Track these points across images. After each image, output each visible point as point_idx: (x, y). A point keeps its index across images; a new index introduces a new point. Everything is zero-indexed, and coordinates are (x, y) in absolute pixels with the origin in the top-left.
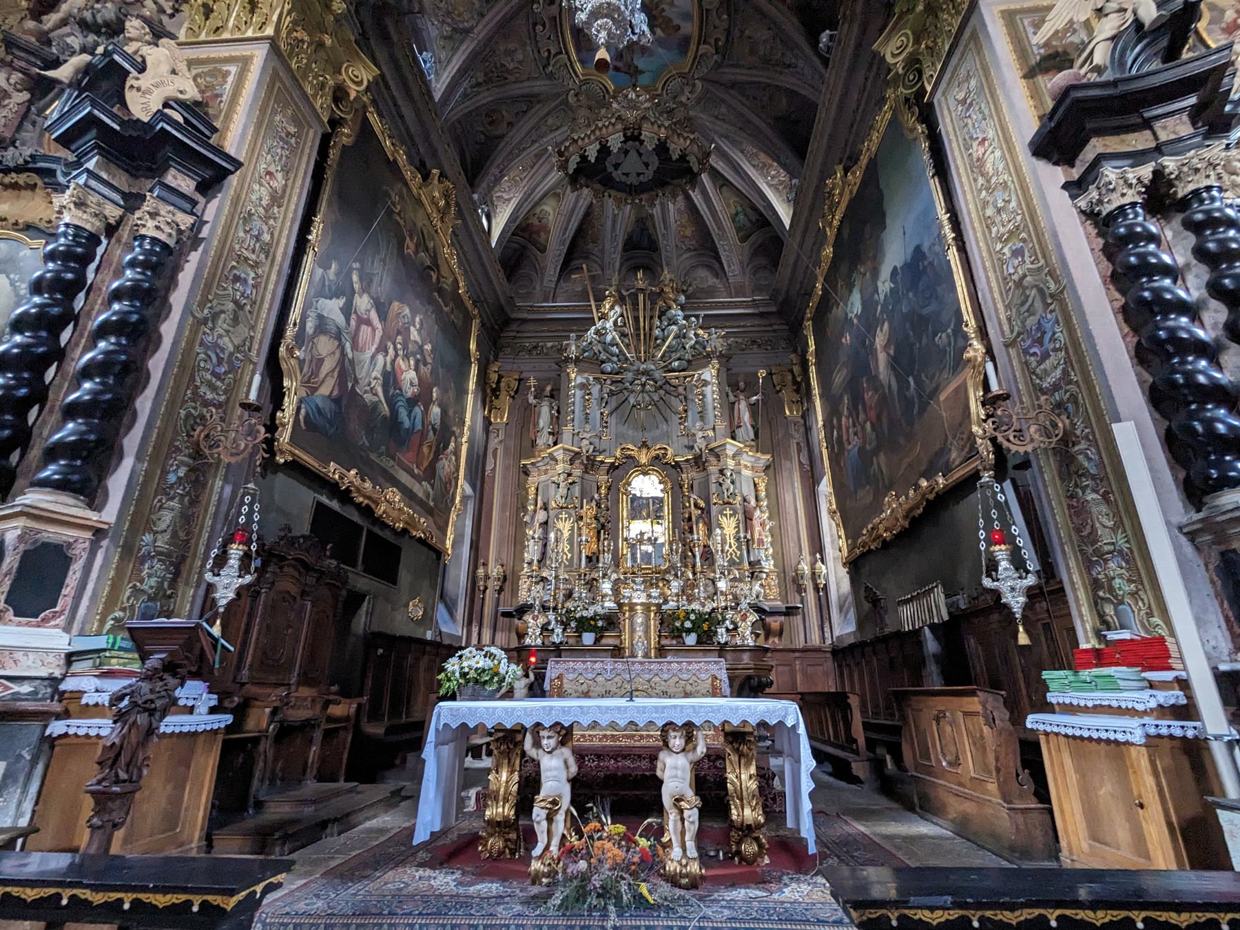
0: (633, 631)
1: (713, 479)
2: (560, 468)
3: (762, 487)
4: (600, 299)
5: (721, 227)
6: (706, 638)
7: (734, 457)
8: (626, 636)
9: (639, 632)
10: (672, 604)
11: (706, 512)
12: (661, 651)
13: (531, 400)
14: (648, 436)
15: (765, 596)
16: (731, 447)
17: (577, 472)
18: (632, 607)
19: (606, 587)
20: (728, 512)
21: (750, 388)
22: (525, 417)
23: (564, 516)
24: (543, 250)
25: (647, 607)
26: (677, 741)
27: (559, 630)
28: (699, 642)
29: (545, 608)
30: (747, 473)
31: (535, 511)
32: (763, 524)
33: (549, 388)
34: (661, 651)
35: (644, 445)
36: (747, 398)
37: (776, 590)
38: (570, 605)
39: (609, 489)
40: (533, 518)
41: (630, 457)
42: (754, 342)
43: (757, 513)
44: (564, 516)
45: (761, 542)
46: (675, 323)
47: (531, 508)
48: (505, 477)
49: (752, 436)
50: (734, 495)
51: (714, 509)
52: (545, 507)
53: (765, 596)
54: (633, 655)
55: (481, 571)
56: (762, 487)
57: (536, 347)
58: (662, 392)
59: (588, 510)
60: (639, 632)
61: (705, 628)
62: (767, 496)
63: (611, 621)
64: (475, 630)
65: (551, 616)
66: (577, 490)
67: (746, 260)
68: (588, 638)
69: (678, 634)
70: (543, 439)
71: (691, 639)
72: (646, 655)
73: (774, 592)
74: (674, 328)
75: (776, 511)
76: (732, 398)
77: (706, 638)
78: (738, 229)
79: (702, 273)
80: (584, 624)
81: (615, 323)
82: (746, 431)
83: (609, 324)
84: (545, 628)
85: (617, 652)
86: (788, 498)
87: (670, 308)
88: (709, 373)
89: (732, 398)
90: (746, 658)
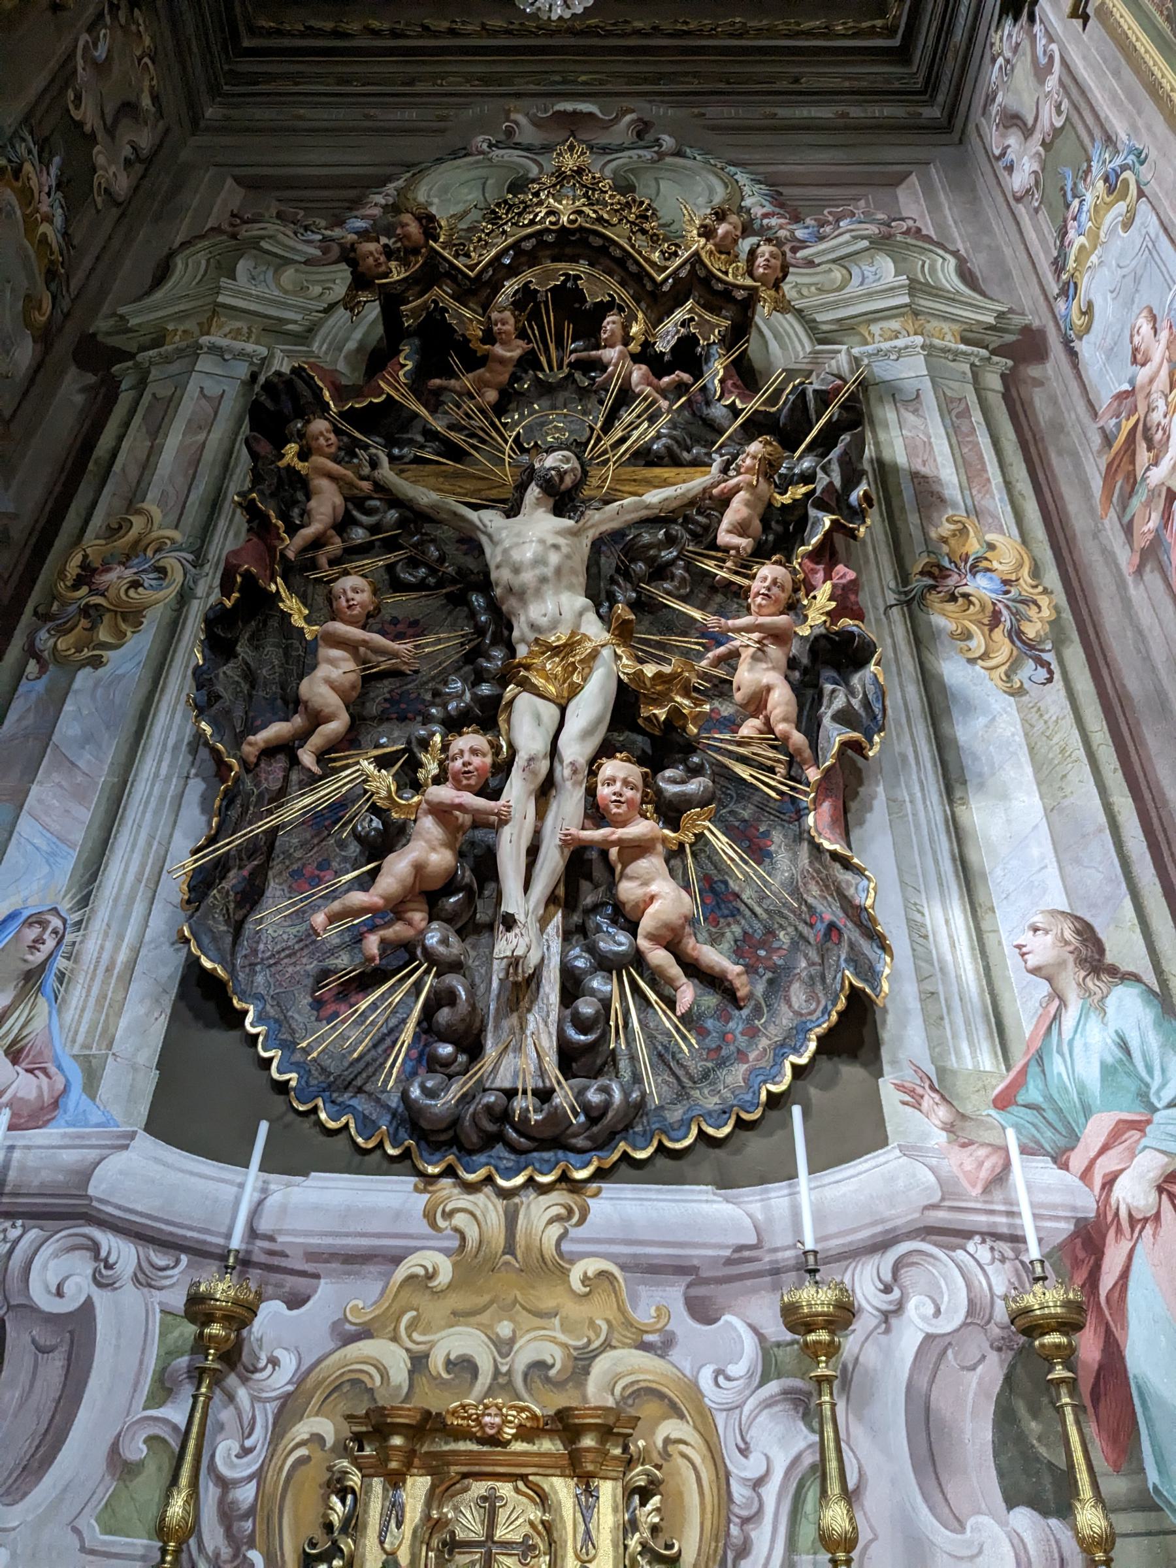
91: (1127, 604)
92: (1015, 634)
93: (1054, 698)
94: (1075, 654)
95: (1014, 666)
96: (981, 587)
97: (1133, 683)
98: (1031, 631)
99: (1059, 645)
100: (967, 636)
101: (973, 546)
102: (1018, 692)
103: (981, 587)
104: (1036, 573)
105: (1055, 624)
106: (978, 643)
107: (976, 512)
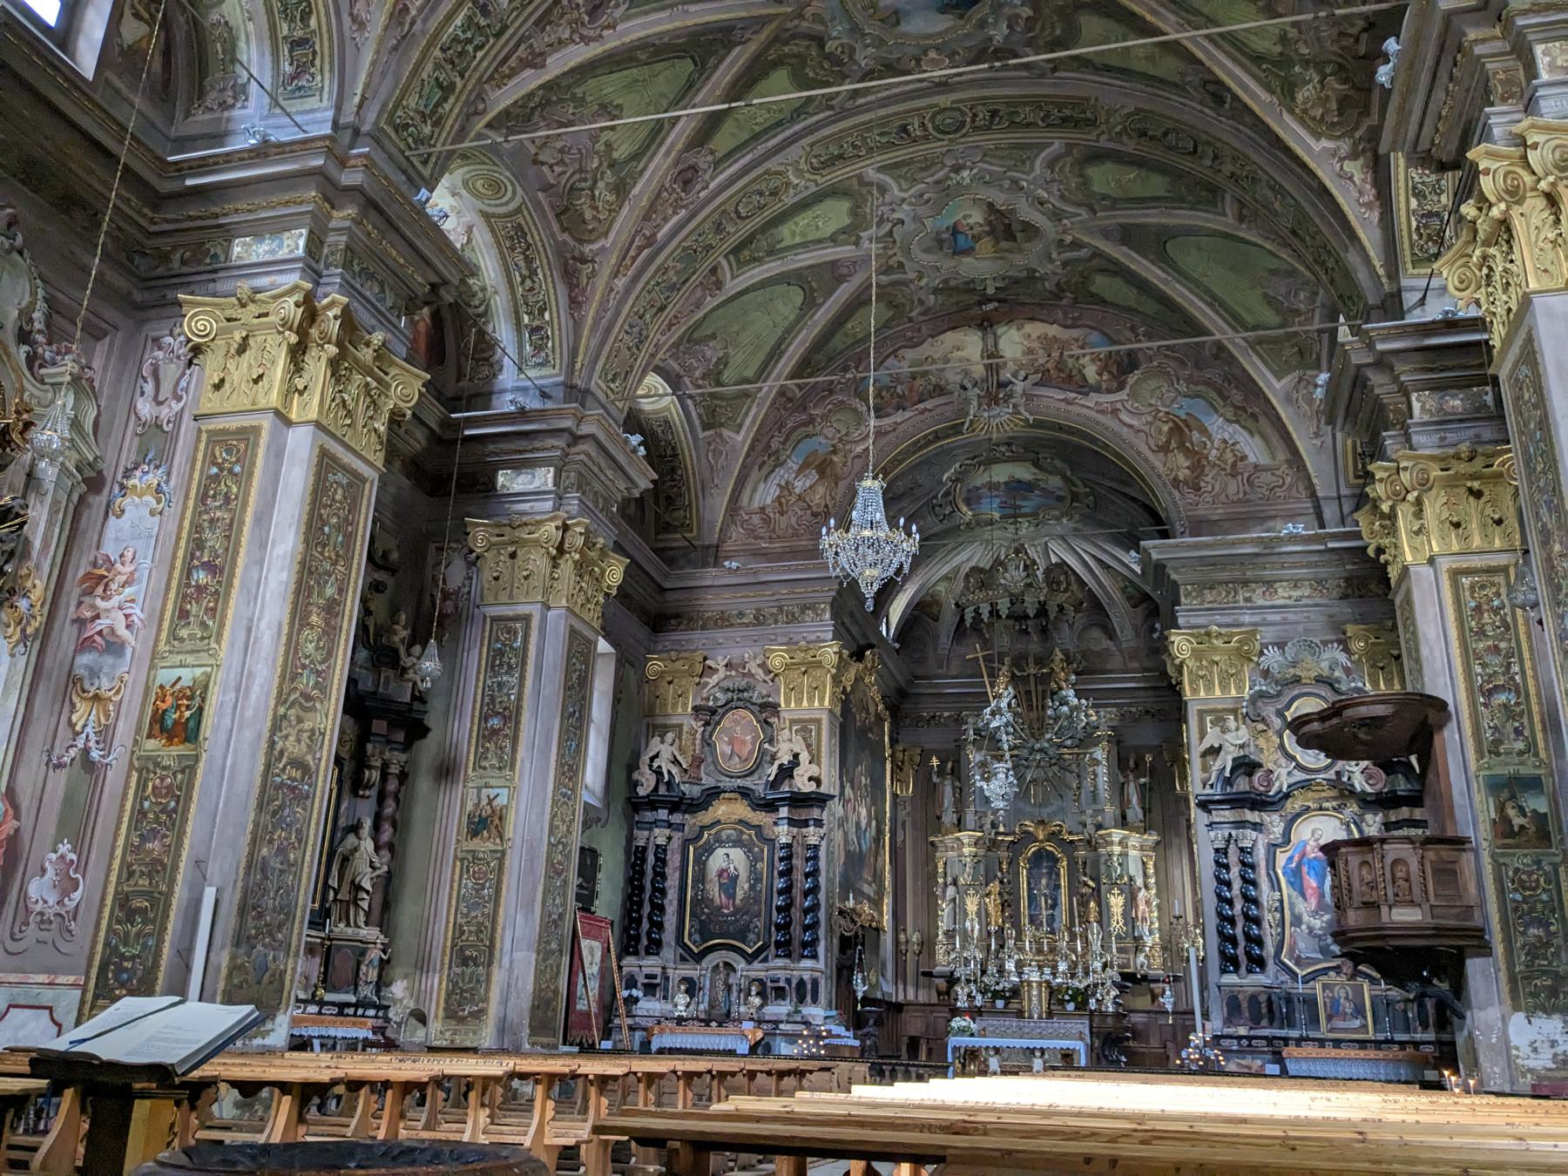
0: (1030, 1000)
1: (1102, 860)
2: (966, 850)
3: (1151, 864)
4: (993, 675)
5: (1110, 598)
6: (1082, 1005)
7: (1120, 843)
8: (1026, 1003)
9: (1035, 1001)
10: (1059, 980)
11: (1097, 890)
12: (1050, 1015)
13: (935, 779)
14: (1046, 811)
15: (1149, 967)
16: (1117, 834)
17: (982, 852)
18: (1030, 983)
19: (1010, 966)
20: (1116, 891)
21: (1138, 769)
22: (928, 791)
23: (972, 892)
24: (936, 619)
25: (1040, 984)
26: (1038, 1054)
27: (979, 997)
28: (1077, 1008)
29: (968, 981)
30: (1133, 853)
31: (946, 885)
32: (1148, 903)
33: (950, 765)
34: (1050, 1015)
35: (1042, 822)
36: (1137, 778)
37: (1159, 961)
38: (985, 979)
39: (1010, 864)
40: (944, 892)
41: (1027, 832)
42: (1147, 712)
43: (1142, 894)
44: (972, 892)
45: (1144, 919)
46: (1067, 703)
47: (941, 881)
48: (914, 849)
49: (1141, 816)
50: (1121, 877)
51: (1103, 888)
52: (955, 883)
53: (1149, 967)
54: (1031, 1017)
55: (902, 937)
56: (1151, 864)
57: (933, 717)
58: (1055, 768)
59: (995, 887)
60: (1035, 1001)
61: (1081, 998)
62: (1156, 873)
63: (1015, 992)
64: (901, 987)
65: (973, 987)
66: (982, 866)
67: (1139, 621)
68: (1000, 1004)
69: (1062, 1002)
70: (949, 818)
71: (1071, 1007)
72: (1040, 1017)
73: (1157, 962)
74: (1065, 709)
75: (1164, 887)
76: (1122, 779)
77: (1082, 1005)
78: (1129, 599)
79: (1096, 633)
80: (997, 995)
81: (1009, 705)
82: (1135, 812)
83: (1004, 704)
84: (969, 995)
85: (1020, 1014)
86: (1177, 873)
87: (1061, 689)
88: (1099, 753)
89: (1122, 779)
90: (1109, 1020)
91: (62, 630)
92: (23, 630)
93: (21, 661)
94: (37, 645)
95: (17, 643)
96: (23, 604)
97: (48, 662)
98: (29, 630)
99: (35, 637)
100: (8, 626)
101: (29, 584)
102: (12, 656)
103: (23, 604)
104: (42, 606)
105: (37, 630)
106: (10, 630)
107: (38, 567)
